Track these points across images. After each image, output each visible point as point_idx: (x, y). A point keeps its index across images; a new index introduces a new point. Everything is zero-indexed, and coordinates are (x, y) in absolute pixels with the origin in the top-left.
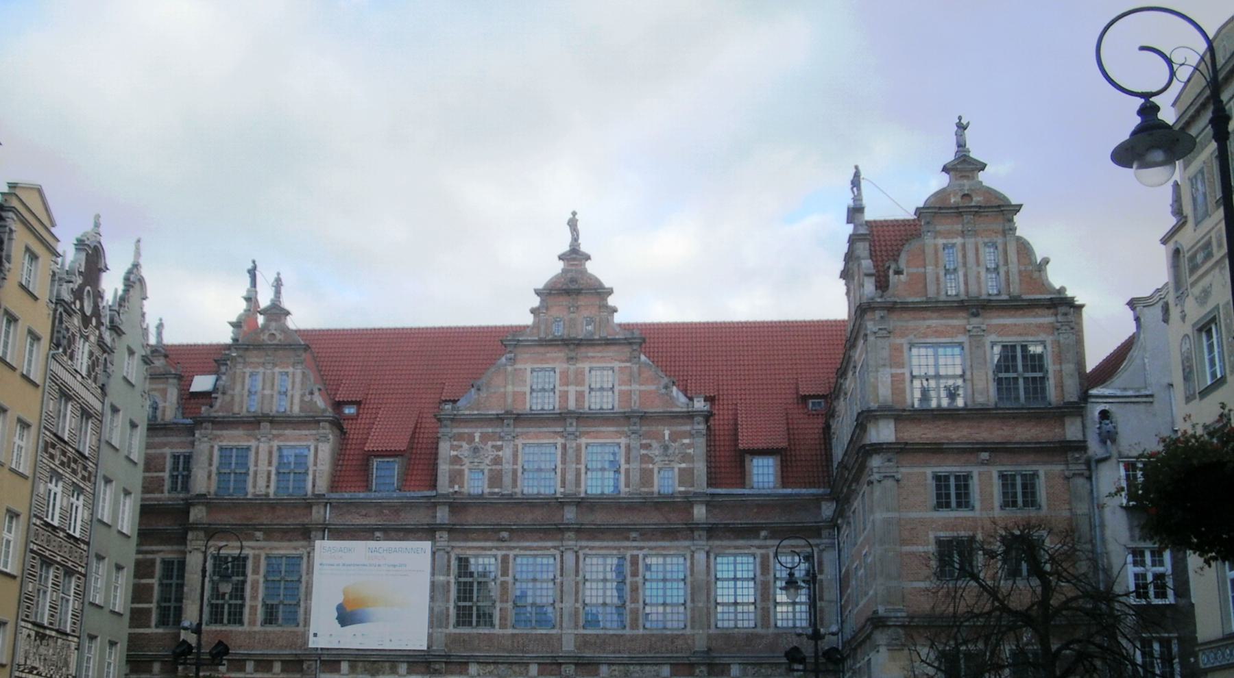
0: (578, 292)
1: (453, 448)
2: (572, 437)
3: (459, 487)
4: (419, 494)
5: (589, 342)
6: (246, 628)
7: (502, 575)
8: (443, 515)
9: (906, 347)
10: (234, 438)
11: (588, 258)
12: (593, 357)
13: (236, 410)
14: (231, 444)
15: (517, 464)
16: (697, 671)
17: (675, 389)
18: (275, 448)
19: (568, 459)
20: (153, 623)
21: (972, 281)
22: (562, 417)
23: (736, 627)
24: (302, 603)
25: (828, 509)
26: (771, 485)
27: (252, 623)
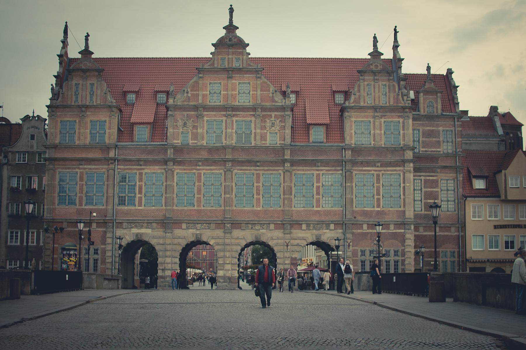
4: (158, 143)
5: (239, 71)
11: (238, 28)
22: (224, 108)
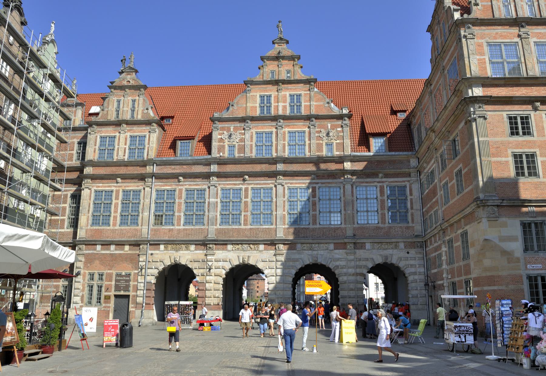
0: (283, 58)
1: (220, 134)
2: (281, 128)
3: (223, 154)
6: (111, 227)
7: (245, 198)
8: (214, 168)
9: (485, 44)
10: (108, 131)
12: (290, 89)
13: (109, 118)
14: (106, 135)
15: (252, 142)
16: (348, 246)
17: (332, 104)
18: (128, 136)
19: (278, 139)
20: (66, 227)
21: (519, 10)
23: (368, 223)
24: (141, 215)
25: (413, 162)
26: (384, 151)
27: (114, 225)
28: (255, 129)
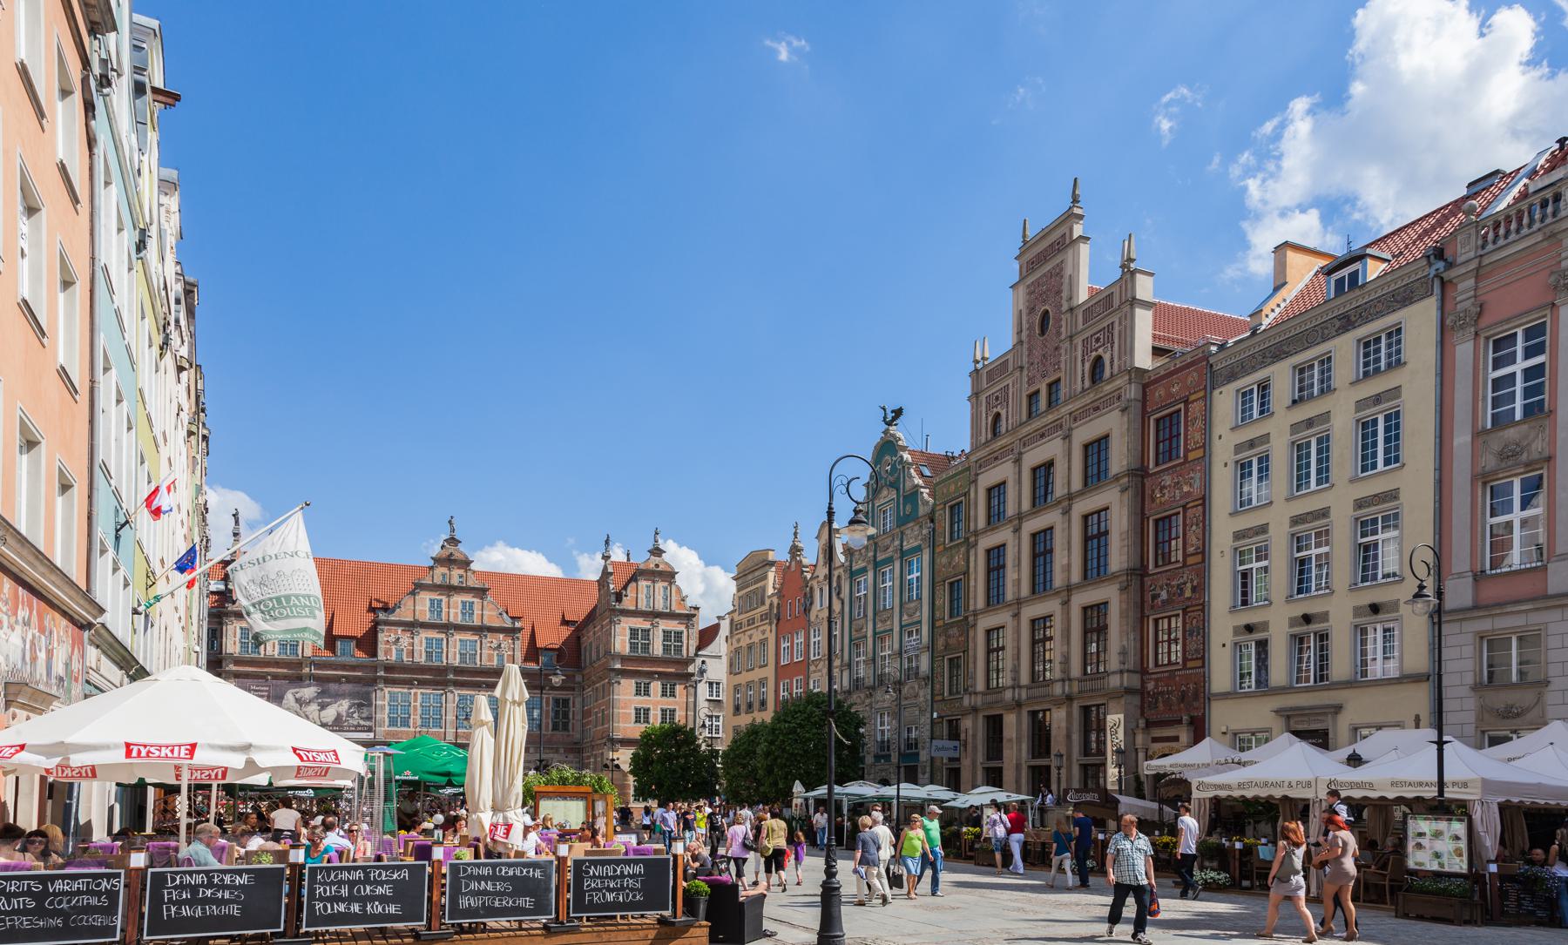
0: (455, 561)
28: (424, 634)
